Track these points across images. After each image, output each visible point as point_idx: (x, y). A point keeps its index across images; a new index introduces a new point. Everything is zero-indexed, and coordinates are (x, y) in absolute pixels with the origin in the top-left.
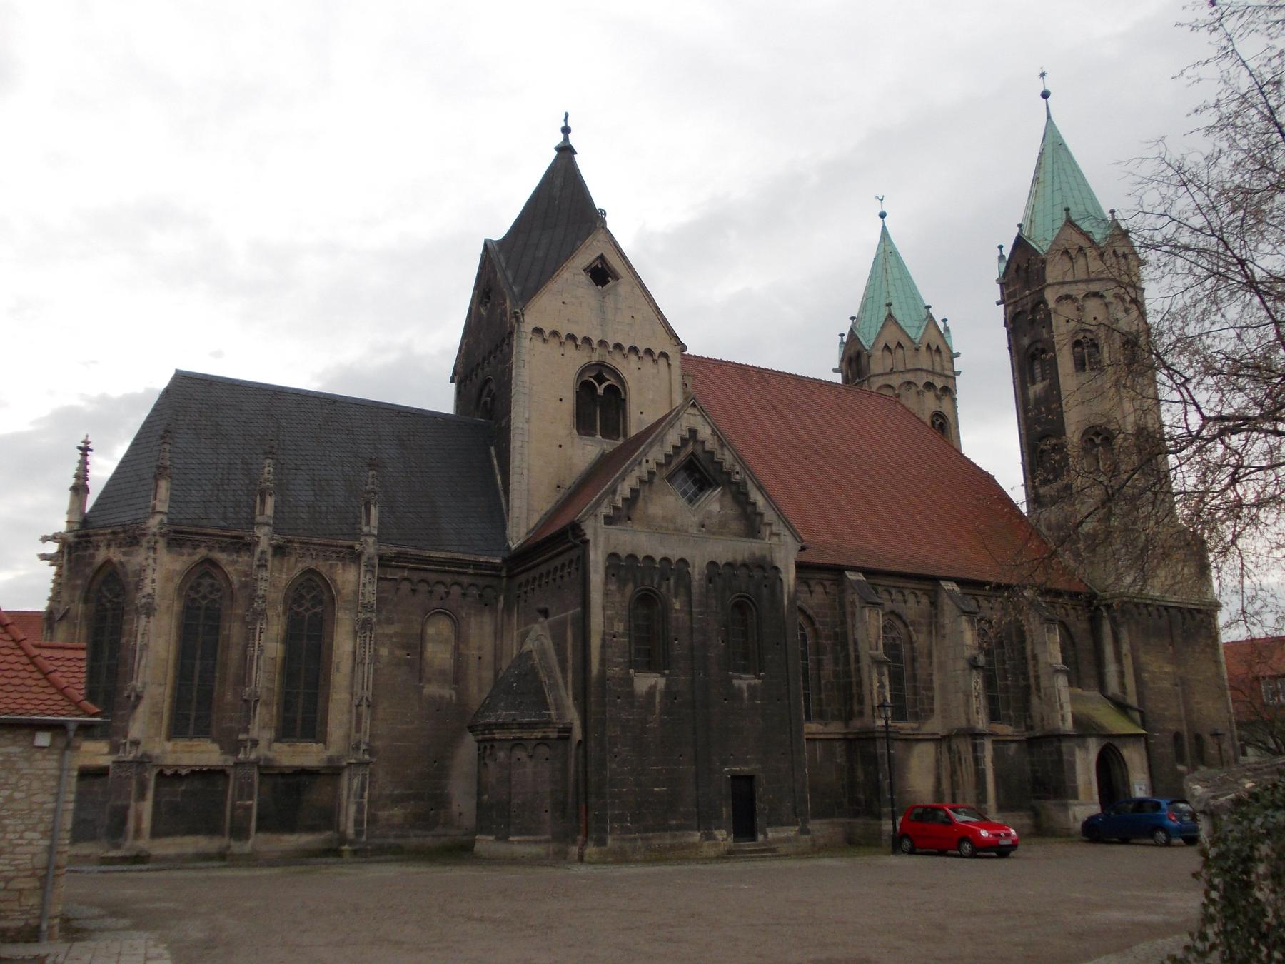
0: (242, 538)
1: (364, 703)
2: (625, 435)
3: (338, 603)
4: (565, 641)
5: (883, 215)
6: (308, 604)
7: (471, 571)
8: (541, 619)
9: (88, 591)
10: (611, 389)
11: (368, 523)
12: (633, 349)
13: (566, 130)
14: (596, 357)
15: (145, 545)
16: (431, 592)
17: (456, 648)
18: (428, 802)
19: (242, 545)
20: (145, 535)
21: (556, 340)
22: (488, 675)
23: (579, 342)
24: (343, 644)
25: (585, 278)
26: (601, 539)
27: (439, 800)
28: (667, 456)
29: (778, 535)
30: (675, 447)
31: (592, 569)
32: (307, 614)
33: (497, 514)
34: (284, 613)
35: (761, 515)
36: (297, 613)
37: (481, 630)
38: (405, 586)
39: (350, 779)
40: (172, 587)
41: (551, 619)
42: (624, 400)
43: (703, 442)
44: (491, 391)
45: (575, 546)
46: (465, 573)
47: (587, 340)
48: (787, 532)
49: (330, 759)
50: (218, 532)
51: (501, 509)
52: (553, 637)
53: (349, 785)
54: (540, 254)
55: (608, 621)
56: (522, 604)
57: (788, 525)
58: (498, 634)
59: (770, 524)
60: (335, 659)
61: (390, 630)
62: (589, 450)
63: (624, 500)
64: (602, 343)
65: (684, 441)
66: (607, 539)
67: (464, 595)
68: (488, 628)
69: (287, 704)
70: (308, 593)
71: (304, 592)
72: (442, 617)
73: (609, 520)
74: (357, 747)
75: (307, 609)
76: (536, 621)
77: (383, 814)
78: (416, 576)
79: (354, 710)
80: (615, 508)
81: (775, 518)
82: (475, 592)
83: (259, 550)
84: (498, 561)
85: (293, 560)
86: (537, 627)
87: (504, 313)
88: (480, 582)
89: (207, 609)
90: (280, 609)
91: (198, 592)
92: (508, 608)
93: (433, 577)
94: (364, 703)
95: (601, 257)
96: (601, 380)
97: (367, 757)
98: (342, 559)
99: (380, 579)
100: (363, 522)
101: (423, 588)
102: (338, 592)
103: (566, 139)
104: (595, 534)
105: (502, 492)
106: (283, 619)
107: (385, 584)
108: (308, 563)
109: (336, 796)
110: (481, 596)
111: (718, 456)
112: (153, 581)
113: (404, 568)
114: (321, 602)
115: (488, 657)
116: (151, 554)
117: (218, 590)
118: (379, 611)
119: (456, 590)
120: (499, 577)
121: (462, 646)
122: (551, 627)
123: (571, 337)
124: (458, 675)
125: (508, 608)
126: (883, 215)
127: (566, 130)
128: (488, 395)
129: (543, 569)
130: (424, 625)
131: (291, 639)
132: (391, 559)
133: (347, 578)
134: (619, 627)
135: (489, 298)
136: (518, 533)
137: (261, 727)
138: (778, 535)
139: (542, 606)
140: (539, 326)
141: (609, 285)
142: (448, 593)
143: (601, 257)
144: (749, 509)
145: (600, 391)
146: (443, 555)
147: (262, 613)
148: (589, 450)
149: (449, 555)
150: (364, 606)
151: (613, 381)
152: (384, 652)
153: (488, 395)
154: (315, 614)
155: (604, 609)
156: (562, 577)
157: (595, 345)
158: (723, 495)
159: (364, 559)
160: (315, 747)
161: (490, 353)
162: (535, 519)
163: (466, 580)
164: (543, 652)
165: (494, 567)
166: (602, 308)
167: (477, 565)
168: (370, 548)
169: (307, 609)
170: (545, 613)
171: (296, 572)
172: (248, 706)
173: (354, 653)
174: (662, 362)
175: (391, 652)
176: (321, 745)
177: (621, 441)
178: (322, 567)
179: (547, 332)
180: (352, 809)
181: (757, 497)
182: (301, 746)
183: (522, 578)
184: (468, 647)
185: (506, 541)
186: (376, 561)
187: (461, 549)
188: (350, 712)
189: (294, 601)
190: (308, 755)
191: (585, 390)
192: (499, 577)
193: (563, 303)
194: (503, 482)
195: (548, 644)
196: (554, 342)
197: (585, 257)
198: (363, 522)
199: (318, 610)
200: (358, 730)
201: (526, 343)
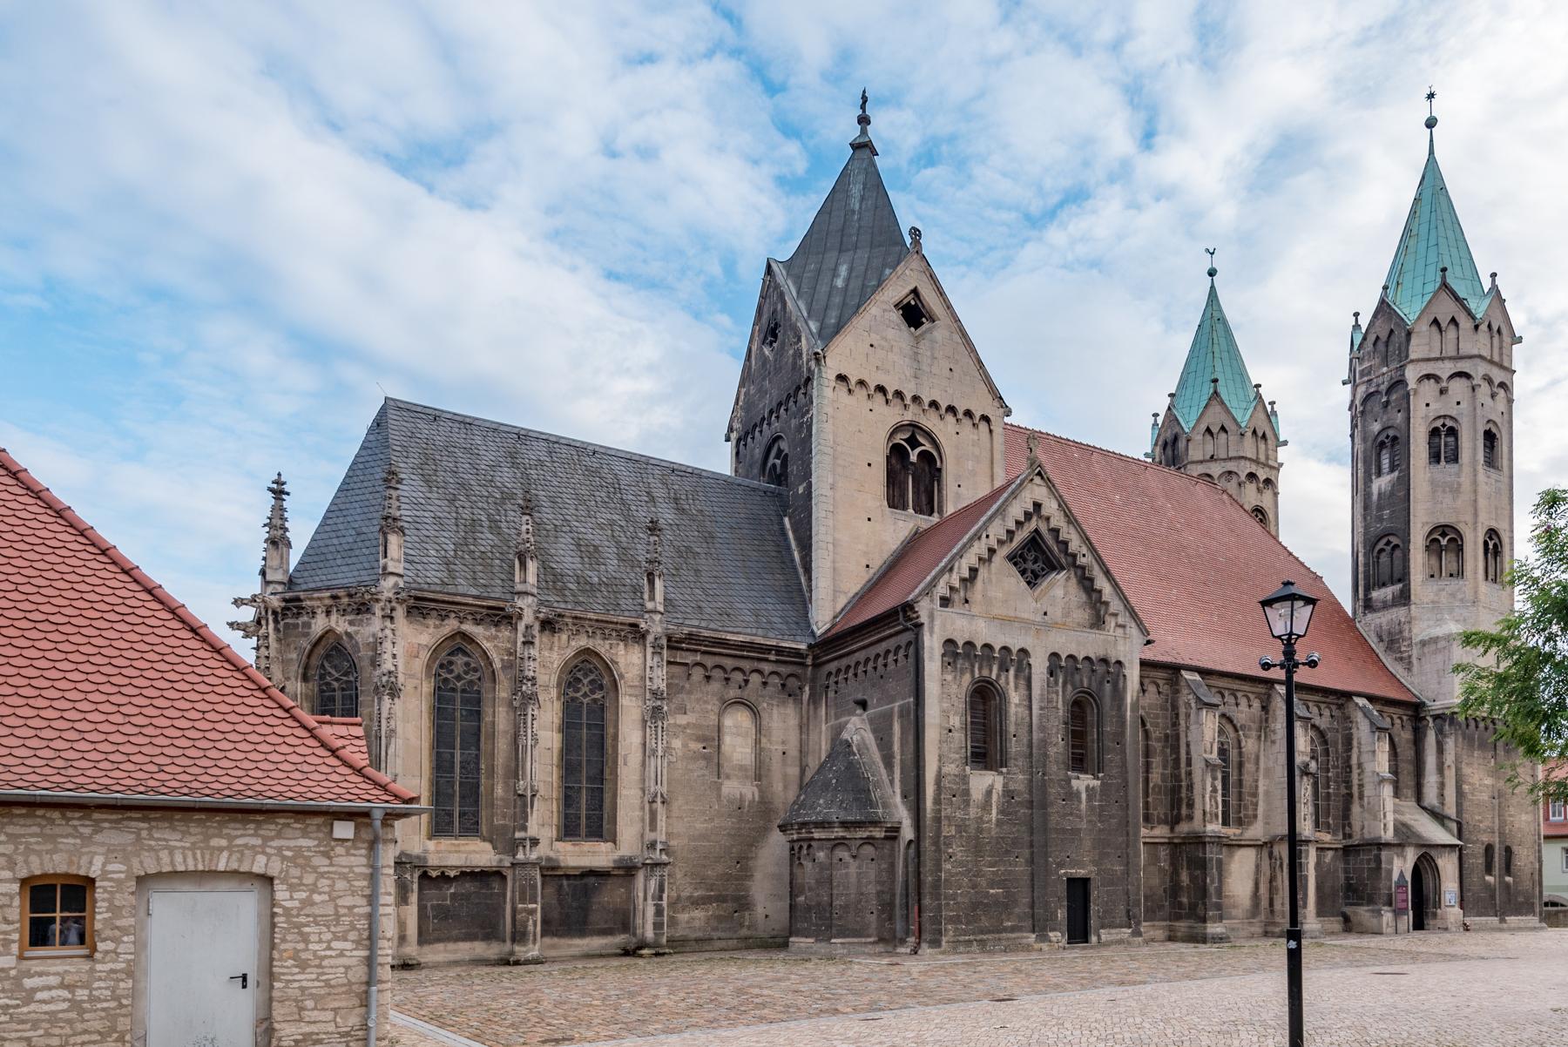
0: (502, 609)
1: (659, 800)
2: (940, 512)
3: (622, 688)
4: (891, 735)
6: (586, 689)
7: (772, 657)
8: (859, 711)
9: (306, 667)
10: (925, 455)
11: (652, 598)
12: (951, 409)
13: (864, 120)
14: (909, 416)
15: (379, 613)
16: (727, 679)
17: (757, 742)
18: (730, 899)
19: (501, 617)
20: (377, 600)
21: (864, 392)
22: (794, 771)
23: (890, 396)
24: (629, 734)
25: (896, 316)
27: (743, 903)
31: (926, 656)
32: (586, 701)
33: (799, 598)
34: (558, 698)
36: (573, 699)
37: (782, 721)
38: (698, 674)
39: (646, 879)
40: (419, 665)
41: (870, 711)
42: (940, 470)
44: (780, 451)
46: (766, 660)
47: (899, 394)
49: (621, 859)
50: (470, 601)
51: (801, 590)
52: (874, 731)
53: (644, 886)
54: (839, 283)
55: (945, 714)
56: (831, 694)
58: (803, 727)
60: (621, 751)
61: (682, 720)
62: (905, 524)
64: (916, 399)
67: (765, 684)
68: (793, 721)
69: (568, 798)
70: (586, 675)
71: (579, 675)
72: (742, 708)
74: (652, 845)
75: (585, 695)
76: (853, 714)
77: (683, 917)
78: (710, 661)
79: (647, 807)
82: (776, 680)
83: (521, 627)
84: (803, 647)
85: (564, 637)
86: (854, 719)
87: (798, 354)
88: (783, 669)
89: (463, 691)
90: (554, 693)
91: (451, 672)
92: (814, 699)
93: (729, 663)
94: (659, 800)
95: (915, 291)
97: (664, 857)
98: (624, 639)
99: (669, 663)
100: (646, 596)
101: (717, 674)
102: (621, 676)
103: (864, 132)
105: (801, 571)
106: (557, 706)
107: (676, 669)
108: (583, 642)
109: (630, 898)
110: (783, 685)
112: (394, 656)
113: (696, 651)
114: (601, 687)
115: (793, 752)
116: (388, 623)
117: (475, 670)
118: (669, 699)
119: (755, 679)
120: (803, 665)
121: (764, 740)
122: (871, 721)
123: (881, 389)
124: (759, 772)
125: (814, 699)
127: (864, 120)
128: (777, 457)
129: (861, 656)
130: (720, 715)
131: (569, 726)
132: (681, 641)
133: (629, 661)
134: (956, 721)
135: (775, 336)
136: (823, 617)
137: (542, 821)
139: (860, 696)
140: (844, 372)
141: (923, 328)
142: (746, 681)
143: (915, 291)
146: (741, 638)
147: (532, 698)
148: (900, 527)
149: (748, 638)
150: (654, 693)
152: (677, 743)
153: (777, 457)
154: (595, 701)
155: (941, 701)
156: (885, 665)
157: (908, 401)
159: (650, 638)
160: (604, 847)
161: (780, 404)
162: (842, 601)
163: (767, 668)
164: (863, 746)
165: (797, 653)
166: (915, 357)
167: (779, 651)
168: (656, 627)
169: (585, 695)
170: (863, 705)
171: (570, 653)
172: (522, 803)
173: (644, 745)
174: (983, 426)
175: (685, 745)
176: (610, 845)
177: (935, 519)
178: (601, 646)
179: (853, 381)
180: (651, 911)
182: (587, 846)
183: (833, 667)
184: (760, 742)
185: (809, 626)
186: (664, 642)
187: (760, 632)
188: (643, 808)
189: (569, 685)
190: (597, 855)
192: (803, 665)
193: (868, 346)
194: (802, 558)
195: (870, 738)
196: (861, 393)
197: (896, 290)
198: (646, 596)
199: (598, 696)
200: (653, 827)
201: (828, 392)
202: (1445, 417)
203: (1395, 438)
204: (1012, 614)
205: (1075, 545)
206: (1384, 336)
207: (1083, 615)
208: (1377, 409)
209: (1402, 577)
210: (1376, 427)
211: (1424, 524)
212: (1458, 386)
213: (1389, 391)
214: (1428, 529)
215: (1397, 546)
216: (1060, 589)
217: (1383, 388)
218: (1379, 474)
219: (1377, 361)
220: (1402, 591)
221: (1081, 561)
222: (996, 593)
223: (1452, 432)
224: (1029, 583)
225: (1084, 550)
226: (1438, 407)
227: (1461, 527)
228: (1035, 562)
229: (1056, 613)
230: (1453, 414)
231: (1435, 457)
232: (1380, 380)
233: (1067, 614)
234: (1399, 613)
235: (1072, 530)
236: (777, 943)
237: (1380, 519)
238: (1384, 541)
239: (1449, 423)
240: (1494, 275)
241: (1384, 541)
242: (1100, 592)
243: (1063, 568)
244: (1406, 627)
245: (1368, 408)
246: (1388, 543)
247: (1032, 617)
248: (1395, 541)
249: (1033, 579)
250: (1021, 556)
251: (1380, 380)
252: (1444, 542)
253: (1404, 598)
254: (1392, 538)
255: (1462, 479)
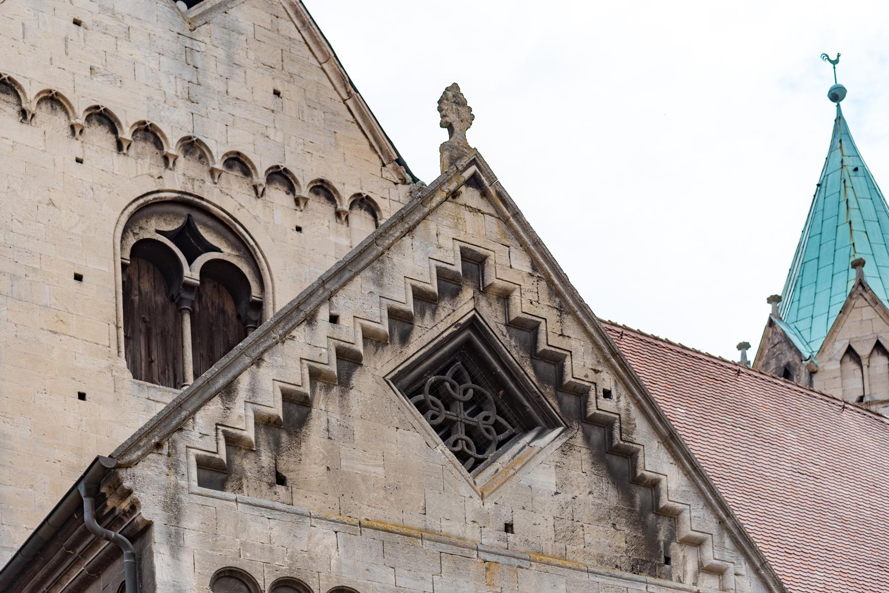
5: (837, 95)
26: (192, 523)
28: (394, 315)
29: (718, 572)
30: (420, 295)
35: (673, 515)
43: (505, 297)
45: (115, 553)
48: (744, 568)
57: (744, 544)
59: (697, 543)
63: (265, 423)
65: (449, 283)
66: (211, 533)
73: (215, 474)
80: (233, 442)
81: (711, 525)
96: (192, 244)
104: (173, 507)
111: (549, 339)
126: (837, 95)
138: (718, 572)
144: (640, 495)
145: (192, 273)
151: (227, 253)
158: (567, 449)
181: (655, 461)
191: (147, 263)
204: (415, 521)
205: (581, 365)
207: (612, 540)
216: (546, 473)
221: (598, 406)
222: (363, 463)
224: (462, 457)
225: (607, 380)
228: (476, 405)
229: (538, 529)
233: (568, 532)
235: (571, 329)
242: (654, 485)
243: (552, 424)
247: (471, 534)
249: (474, 451)
250: (435, 389)
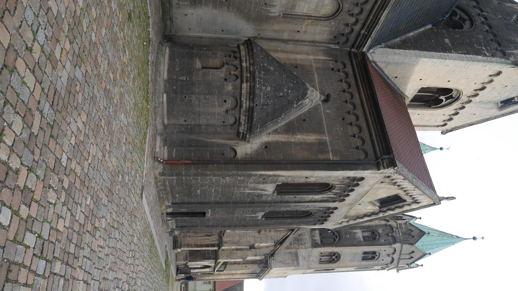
202: (379, 256)
203: (375, 238)
206: (412, 234)
208: (387, 231)
209: (323, 244)
210: (380, 231)
211: (342, 251)
212: (389, 259)
213: (393, 236)
214: (340, 252)
215: (335, 240)
217: (394, 234)
218: (362, 232)
219: (404, 230)
220: (318, 243)
223: (373, 258)
226: (383, 254)
227: (338, 263)
230: (380, 259)
231: (365, 253)
232: (397, 233)
234: (309, 244)
236: (169, 37)
237: (346, 234)
238: (338, 235)
239: (376, 257)
240: (422, 265)
241: (338, 235)
244: (303, 247)
245: (388, 227)
246: (337, 237)
248: (337, 240)
251: (397, 233)
252: (334, 257)
253: (315, 245)
254: (338, 238)
255: (355, 262)
